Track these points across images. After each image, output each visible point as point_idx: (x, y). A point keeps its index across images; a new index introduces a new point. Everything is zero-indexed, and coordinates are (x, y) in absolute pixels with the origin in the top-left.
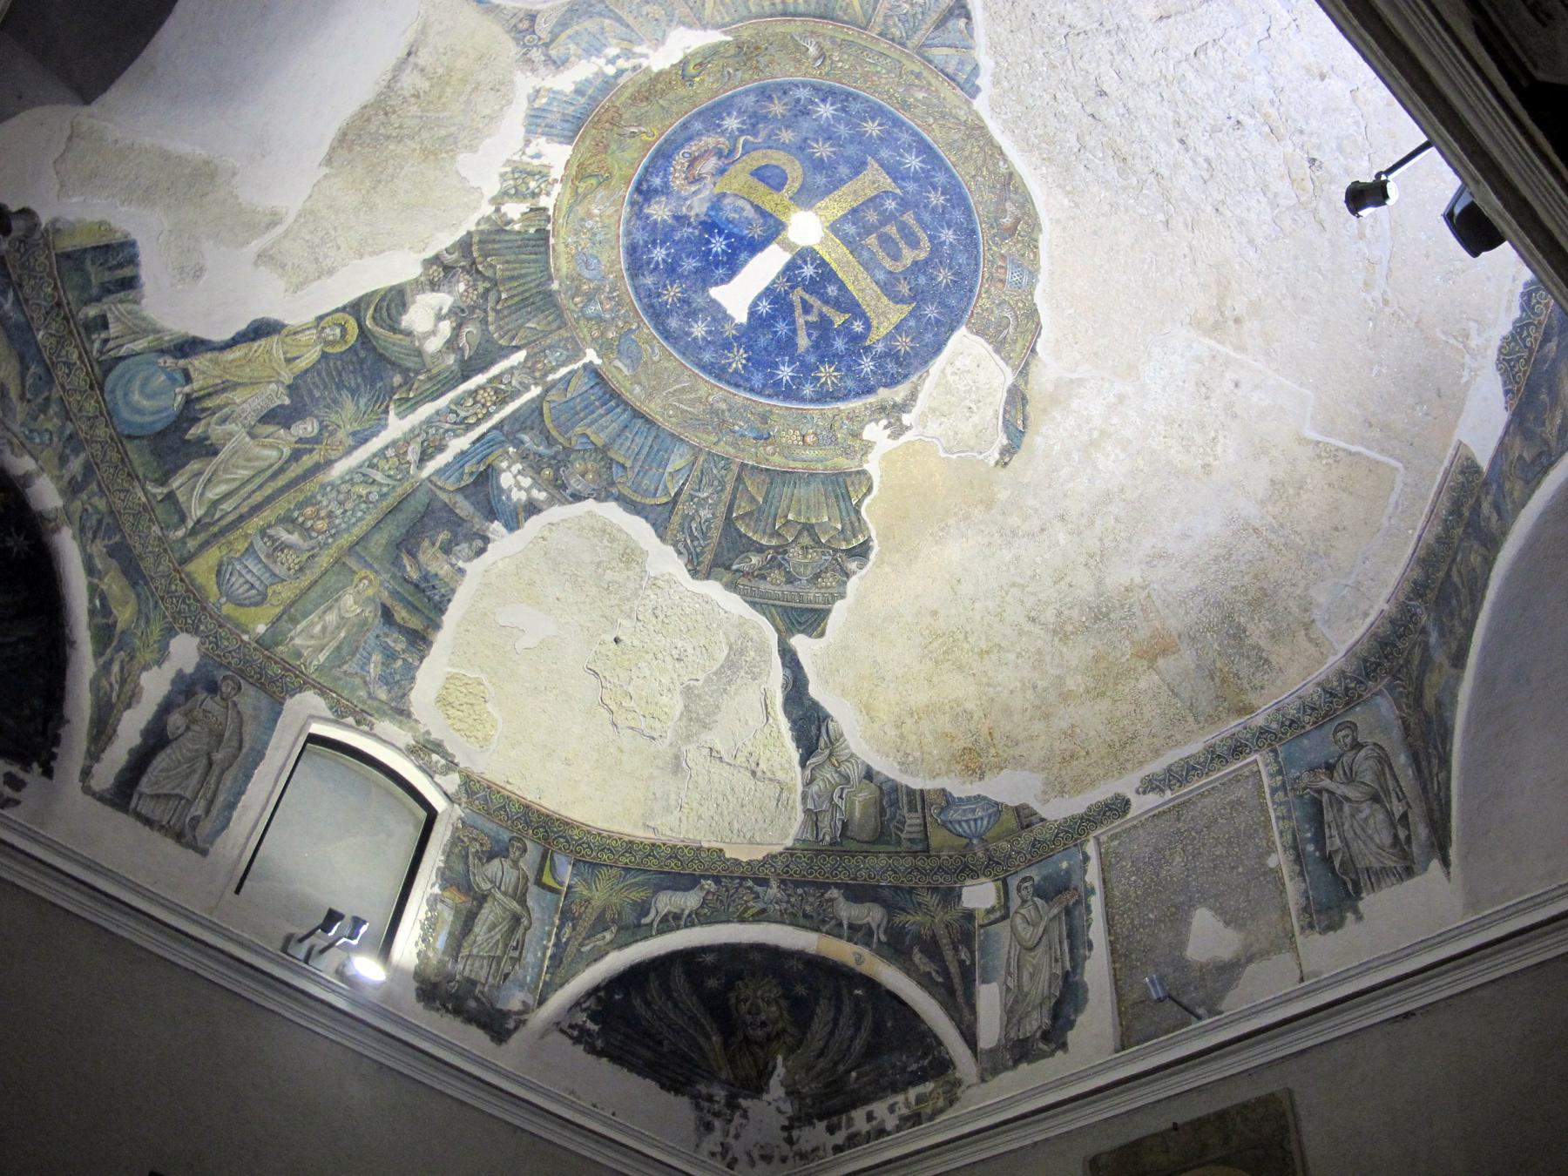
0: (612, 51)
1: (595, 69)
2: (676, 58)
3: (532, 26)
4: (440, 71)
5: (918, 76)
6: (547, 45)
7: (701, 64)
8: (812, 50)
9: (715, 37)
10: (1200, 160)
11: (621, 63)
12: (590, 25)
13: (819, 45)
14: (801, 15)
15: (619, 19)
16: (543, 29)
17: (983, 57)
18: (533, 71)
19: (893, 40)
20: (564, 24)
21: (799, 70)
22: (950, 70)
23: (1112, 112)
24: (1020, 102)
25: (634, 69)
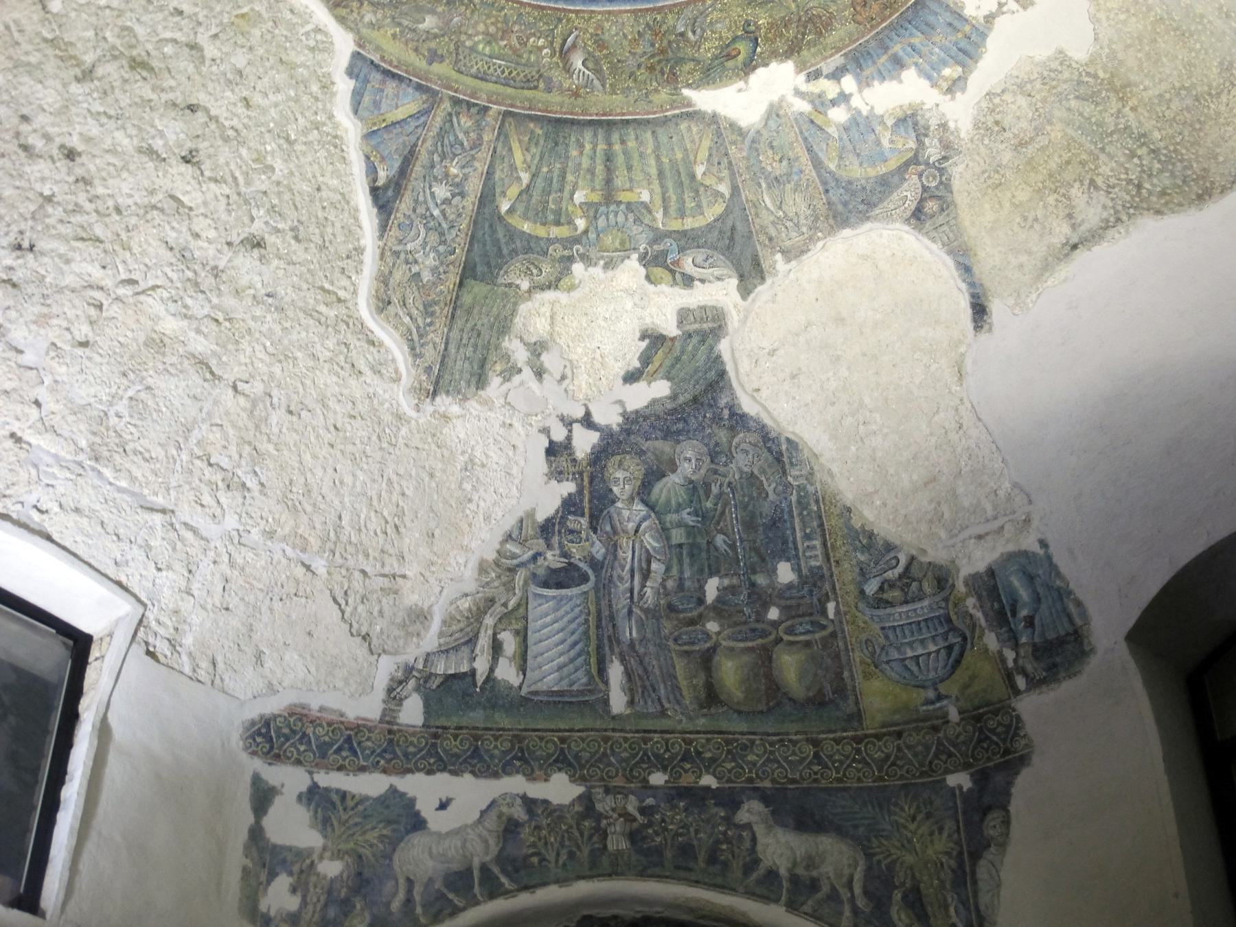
0: (838, 115)
1: (866, 92)
2: (760, 75)
3: (922, 200)
4: (1051, 199)
5: (434, 57)
6: (915, 160)
7: (730, 57)
8: (577, 62)
9: (705, 99)
10: (38, 143)
11: (829, 88)
12: (857, 171)
13: (568, 69)
14: (591, 123)
15: (817, 164)
16: (909, 192)
17: (351, 129)
18: (943, 126)
19: (470, 105)
20: (886, 184)
21: (600, 27)
22: (391, 86)
23: (171, 138)
24: (292, 66)
25: (817, 75)
